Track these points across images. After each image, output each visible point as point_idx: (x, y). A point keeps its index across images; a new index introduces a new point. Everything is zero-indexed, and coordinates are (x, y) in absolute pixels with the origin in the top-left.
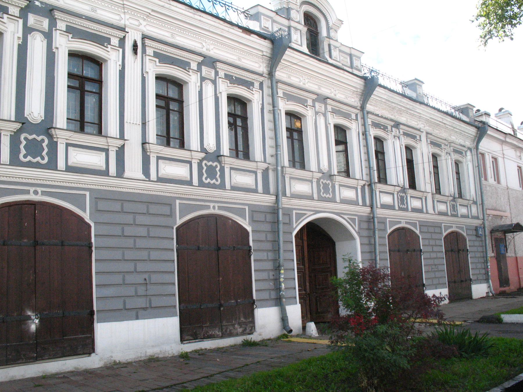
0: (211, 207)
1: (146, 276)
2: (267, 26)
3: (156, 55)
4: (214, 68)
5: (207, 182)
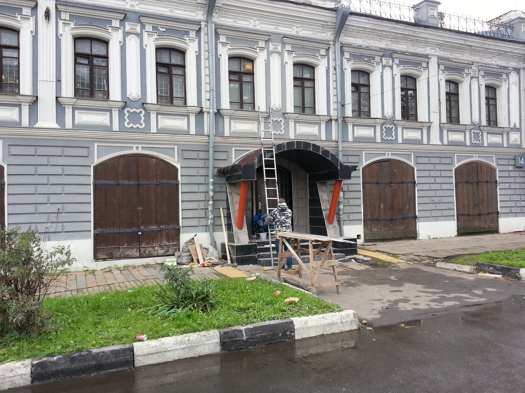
1: (60, 206)
3: (73, 17)
5: (130, 126)
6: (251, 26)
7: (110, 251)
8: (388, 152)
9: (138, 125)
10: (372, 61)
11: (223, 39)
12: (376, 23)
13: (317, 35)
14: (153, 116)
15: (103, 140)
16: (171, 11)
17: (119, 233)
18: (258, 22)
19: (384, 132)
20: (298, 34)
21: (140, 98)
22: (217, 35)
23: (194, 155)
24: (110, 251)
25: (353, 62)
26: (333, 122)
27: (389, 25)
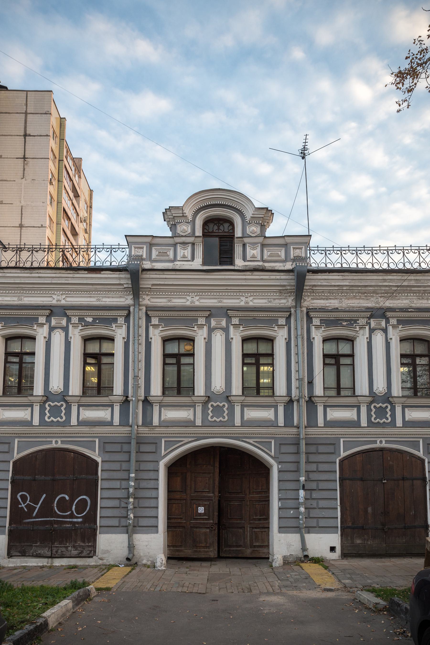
0: (54, 442)
2: (140, 254)
4: (66, 315)
6: (188, 303)
7: (23, 548)
8: (380, 439)
9: (59, 418)
10: (354, 325)
11: (155, 321)
12: (355, 278)
13: (274, 302)
14: (74, 409)
15: (23, 435)
16: (98, 300)
17: (33, 530)
18: (197, 298)
19: (372, 413)
20: (248, 305)
21: (62, 390)
22: (148, 318)
23: (117, 448)
24: (23, 548)
25: (323, 329)
26: (295, 404)
27: (375, 277)
